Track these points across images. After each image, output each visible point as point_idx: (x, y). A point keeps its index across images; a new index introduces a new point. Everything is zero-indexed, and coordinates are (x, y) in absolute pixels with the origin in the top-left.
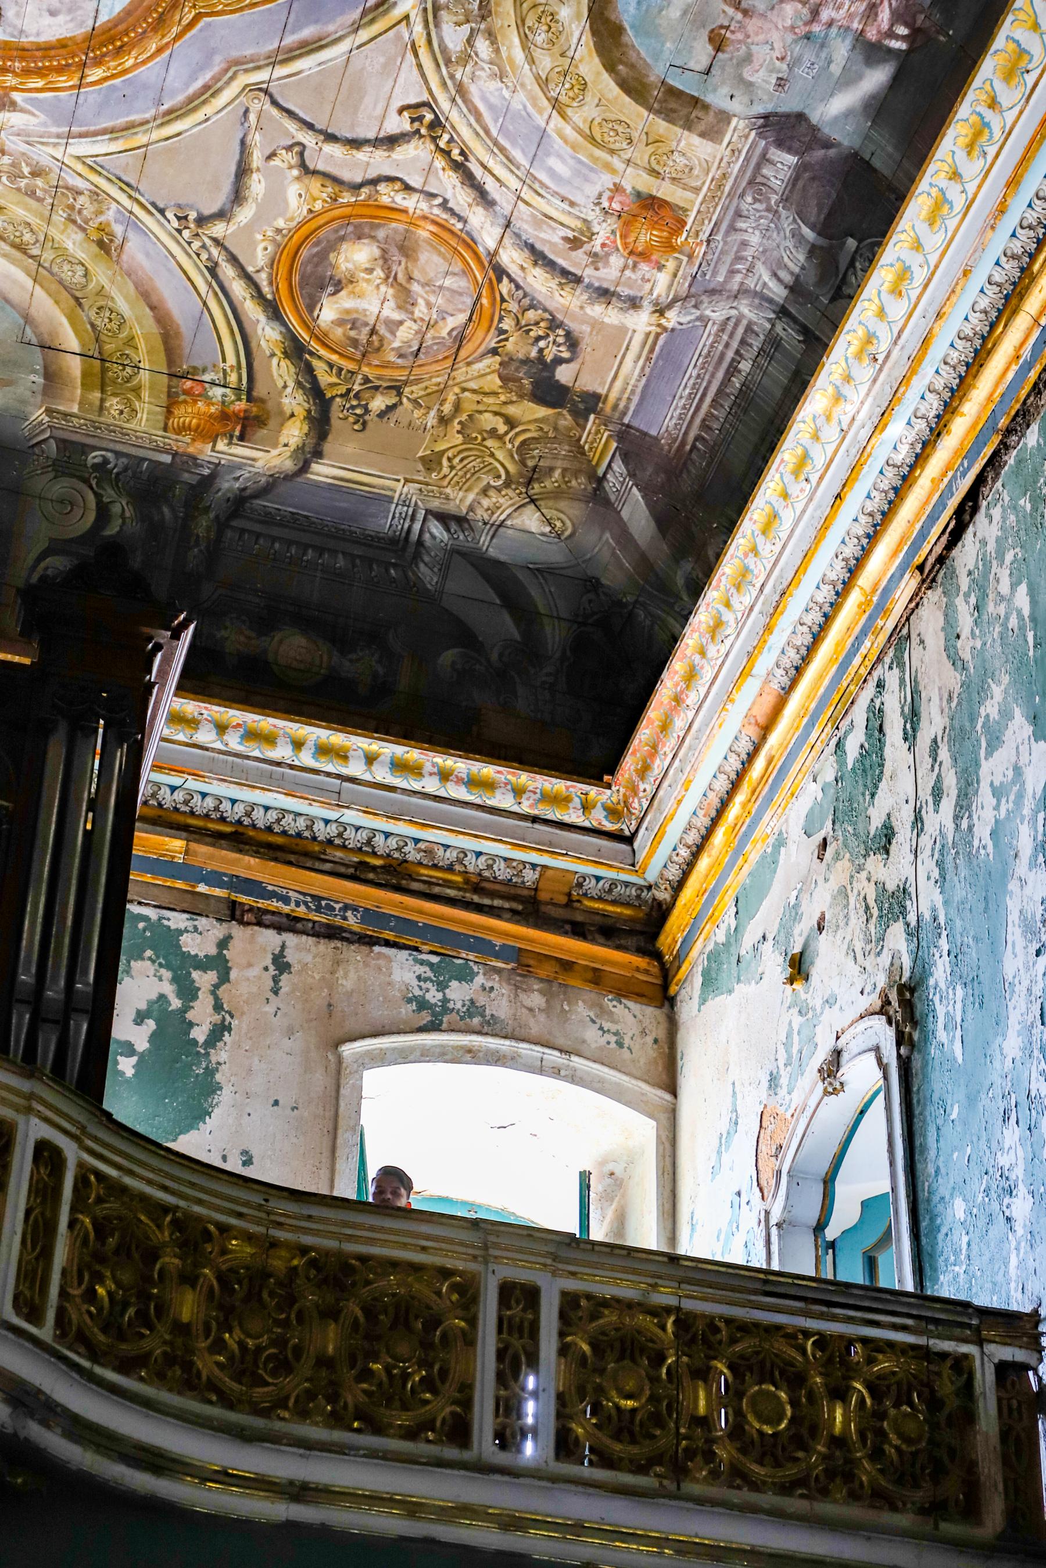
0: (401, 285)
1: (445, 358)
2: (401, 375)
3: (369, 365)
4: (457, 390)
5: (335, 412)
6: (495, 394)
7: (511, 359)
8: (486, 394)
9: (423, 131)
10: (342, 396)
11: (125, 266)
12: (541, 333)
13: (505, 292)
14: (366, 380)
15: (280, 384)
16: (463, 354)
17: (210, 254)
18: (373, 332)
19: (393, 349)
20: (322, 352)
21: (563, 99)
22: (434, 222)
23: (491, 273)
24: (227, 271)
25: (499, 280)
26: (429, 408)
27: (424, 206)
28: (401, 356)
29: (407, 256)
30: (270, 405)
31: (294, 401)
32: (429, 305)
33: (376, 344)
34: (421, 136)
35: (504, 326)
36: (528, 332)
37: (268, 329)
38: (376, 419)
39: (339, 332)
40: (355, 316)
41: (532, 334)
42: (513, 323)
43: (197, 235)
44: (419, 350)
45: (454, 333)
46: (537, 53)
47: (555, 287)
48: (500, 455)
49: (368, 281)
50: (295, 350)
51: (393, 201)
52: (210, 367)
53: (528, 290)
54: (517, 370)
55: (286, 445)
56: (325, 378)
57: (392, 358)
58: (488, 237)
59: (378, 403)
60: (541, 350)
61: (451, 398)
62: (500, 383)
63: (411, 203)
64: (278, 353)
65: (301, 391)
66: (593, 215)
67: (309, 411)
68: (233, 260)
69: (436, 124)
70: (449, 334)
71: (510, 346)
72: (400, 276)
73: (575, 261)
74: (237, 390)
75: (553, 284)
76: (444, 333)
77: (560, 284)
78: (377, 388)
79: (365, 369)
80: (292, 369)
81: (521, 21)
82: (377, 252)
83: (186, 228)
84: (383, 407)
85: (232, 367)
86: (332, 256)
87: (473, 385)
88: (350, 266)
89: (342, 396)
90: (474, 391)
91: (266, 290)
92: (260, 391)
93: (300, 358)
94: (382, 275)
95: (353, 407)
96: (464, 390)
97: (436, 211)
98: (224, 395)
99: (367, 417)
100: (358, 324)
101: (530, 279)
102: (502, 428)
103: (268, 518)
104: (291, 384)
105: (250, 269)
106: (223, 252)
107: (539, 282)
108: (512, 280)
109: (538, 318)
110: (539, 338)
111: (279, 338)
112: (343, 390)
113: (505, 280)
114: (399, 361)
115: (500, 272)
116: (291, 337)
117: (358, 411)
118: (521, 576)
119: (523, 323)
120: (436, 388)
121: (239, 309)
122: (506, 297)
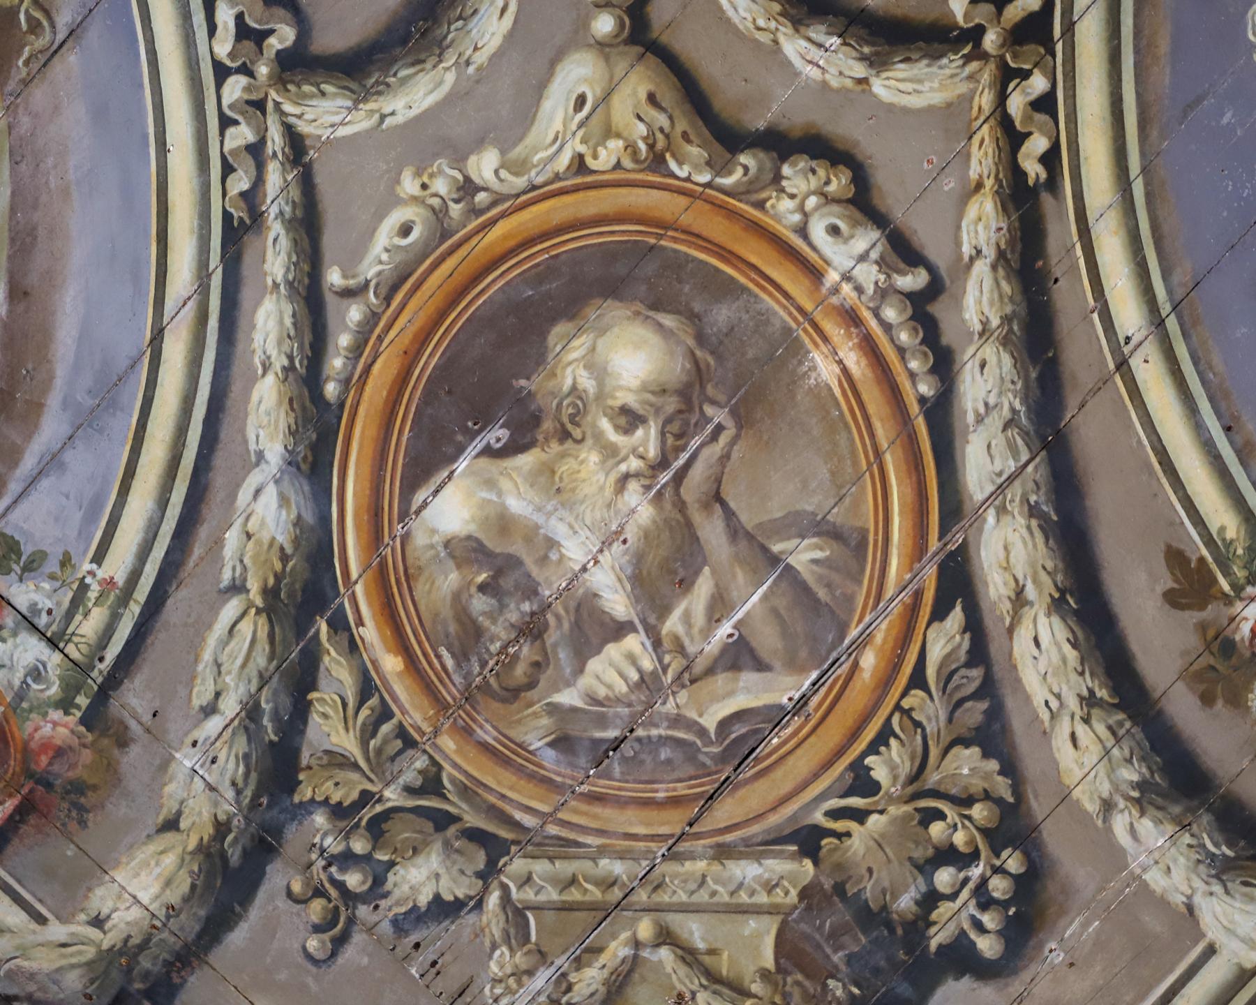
0: (681, 506)
1: (675, 802)
2: (526, 803)
3: (466, 732)
4: (645, 929)
5: (280, 878)
7: (840, 889)
8: (714, 978)
10: (339, 812)
11: (25, 122)
12: (959, 839)
13: (935, 654)
14: (431, 784)
15: (202, 694)
16: (726, 811)
17: (259, 181)
18: (532, 629)
19: (553, 709)
20: (370, 632)
22: (869, 346)
23: (930, 574)
24: (274, 257)
25: (939, 614)
26: (542, 957)
28: (562, 743)
30: (133, 759)
31: (200, 776)
32: (719, 607)
33: (520, 670)
35: (880, 773)
37: (271, 493)
38: (386, 927)
39: (451, 579)
40: (517, 548)
41: (937, 830)
42: (905, 769)
43: (260, 105)
44: (617, 744)
45: (739, 730)
47: (1073, 703)
50: (303, 597)
52: (52, 566)
53: (999, 670)
54: (834, 936)
55: (98, 922)
56: (329, 730)
57: (535, 734)
58: (984, 458)
59: (422, 876)
60: (931, 899)
61: (618, 950)
62: (768, 959)
64: (254, 586)
65: (241, 745)
67: (222, 828)
68: (308, 224)
70: (725, 724)
71: (860, 839)
72: (698, 473)
73: (1160, 641)
74: (81, 669)
75: (1073, 687)
77: (1089, 701)
78: (442, 821)
79: (448, 743)
80: (260, 660)
82: (677, 370)
83: (246, 70)
84: (424, 899)
85: (111, 582)
86: (559, 330)
87: (695, 931)
88: (587, 383)
89: (339, 812)
90: (688, 955)
91: (336, 363)
92: (135, 699)
93: (302, 625)
94: (652, 452)
95: (347, 859)
96: (665, 937)
98: (36, 673)
99: (363, 911)
100: (507, 583)
101: (1022, 644)
104: (230, 706)
105: (334, 277)
106: (295, 193)
107: (1043, 659)
108: (975, 626)
109: (977, 785)
110: (947, 855)
111: (283, 538)
112: (345, 790)
113: (956, 617)
114: (549, 757)
115: (957, 582)
116: (316, 547)
117: (354, 880)
119: (932, 778)
120: (595, 893)
121: (236, 388)
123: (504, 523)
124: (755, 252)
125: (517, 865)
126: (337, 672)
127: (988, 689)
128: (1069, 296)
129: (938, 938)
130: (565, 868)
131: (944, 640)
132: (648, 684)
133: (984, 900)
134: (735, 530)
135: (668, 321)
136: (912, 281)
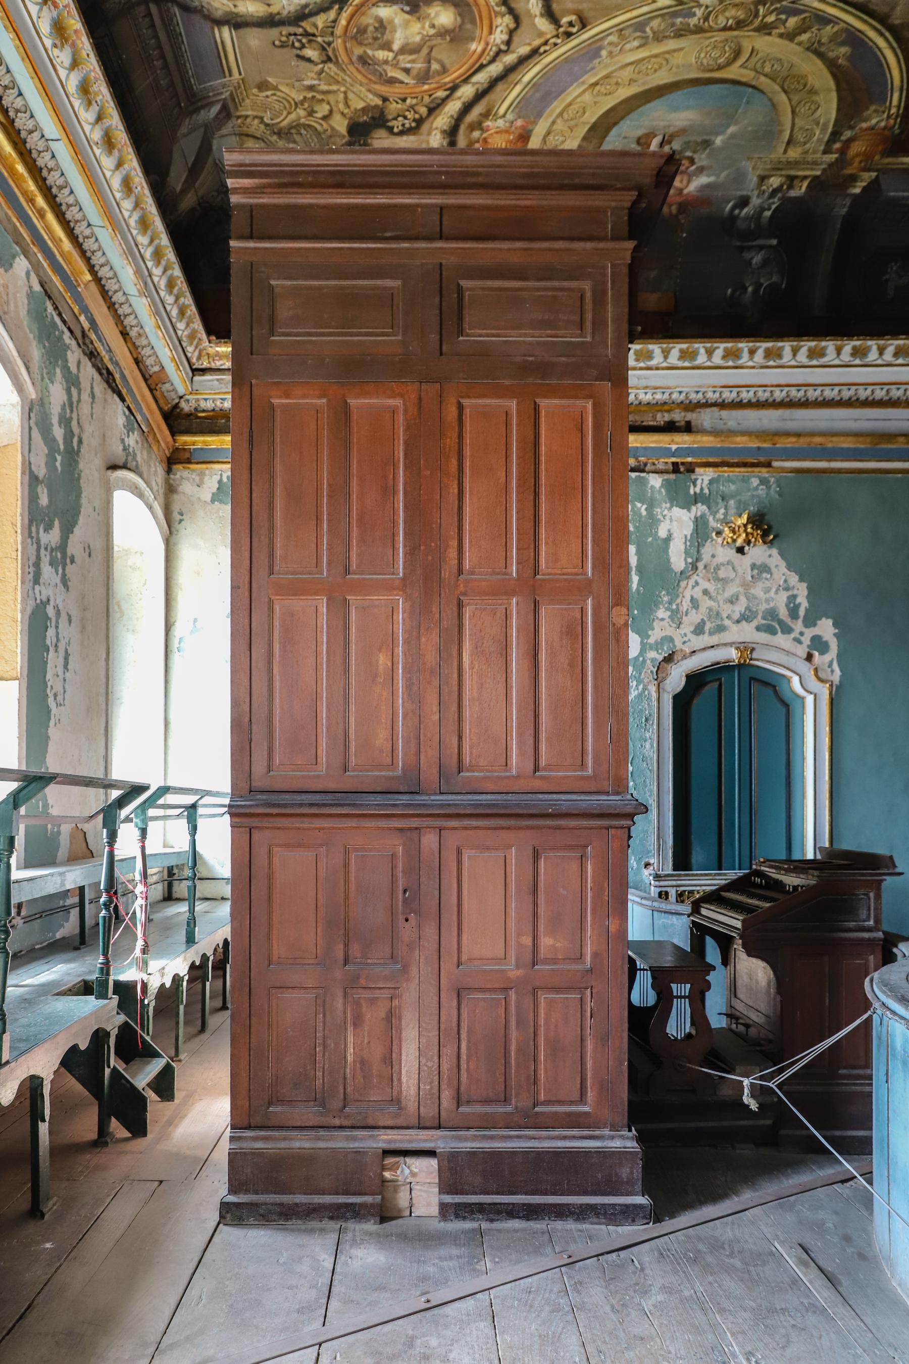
0: (425, 43)
3: (345, 42)
4: (343, 89)
6: (349, 107)
9: (561, 30)
20: (345, 15)
21: (598, 88)
22: (484, 50)
23: (451, 85)
25: (446, 90)
26: (320, 80)
27: (498, 41)
29: (451, 41)
32: (413, 61)
34: (557, 30)
35: (409, 101)
36: (408, 110)
39: (371, 21)
41: (407, 113)
46: (631, 68)
48: (293, 116)
49: (423, 28)
51: (497, 27)
63: (499, 36)
66: (510, 116)
69: (568, 35)
76: (390, 74)
79: (340, 41)
81: (656, 56)
87: (351, 95)
88: (433, 15)
90: (346, 98)
97: (494, 49)
102: (319, 115)
103: (168, 22)
108: (448, 97)
115: (454, 88)
118: (210, 160)
122: (433, 96)
123: (391, 21)
124: (486, 23)
125: (331, 65)
126: (332, 14)
127: (439, 105)
128: (523, 69)
129: (390, 124)
130: (339, 72)
131: (441, 94)
132: (386, 62)
133: (403, 125)
134: (429, 54)
135: (459, 19)
136: (503, 47)
